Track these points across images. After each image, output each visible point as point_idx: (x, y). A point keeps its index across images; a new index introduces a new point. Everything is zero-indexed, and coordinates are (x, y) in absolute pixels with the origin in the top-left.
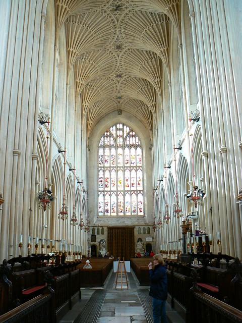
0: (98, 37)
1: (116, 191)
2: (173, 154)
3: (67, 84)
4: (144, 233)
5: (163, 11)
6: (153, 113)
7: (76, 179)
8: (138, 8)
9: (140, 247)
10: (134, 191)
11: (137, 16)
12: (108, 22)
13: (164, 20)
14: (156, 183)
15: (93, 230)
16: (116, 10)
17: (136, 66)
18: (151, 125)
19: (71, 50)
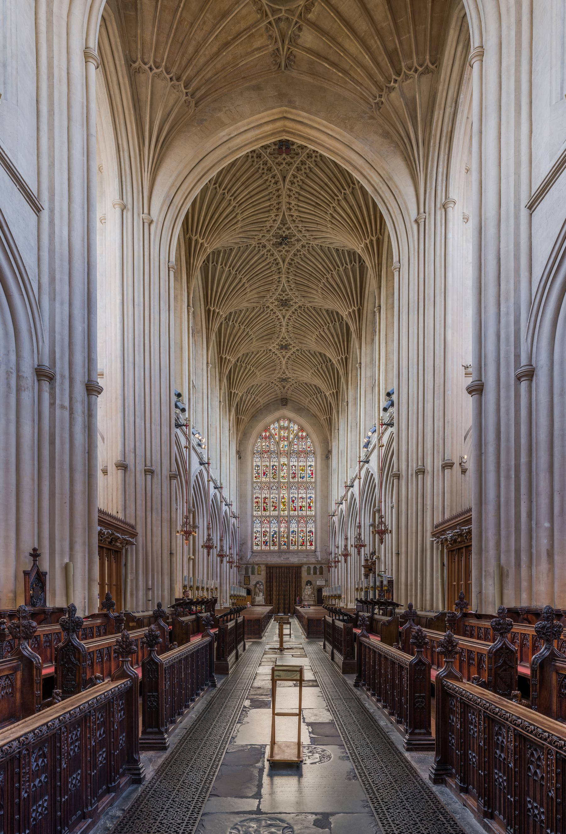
0: (253, 287)
1: (277, 517)
2: (357, 468)
3: (207, 363)
4: (315, 573)
5: (356, 249)
6: (333, 405)
7: (223, 500)
8: (317, 242)
9: (309, 593)
10: (302, 517)
11: (314, 253)
12: (268, 264)
13: (357, 262)
14: (334, 507)
15: (247, 569)
16: (281, 244)
17: (311, 334)
18: (330, 421)
19: (212, 309)
